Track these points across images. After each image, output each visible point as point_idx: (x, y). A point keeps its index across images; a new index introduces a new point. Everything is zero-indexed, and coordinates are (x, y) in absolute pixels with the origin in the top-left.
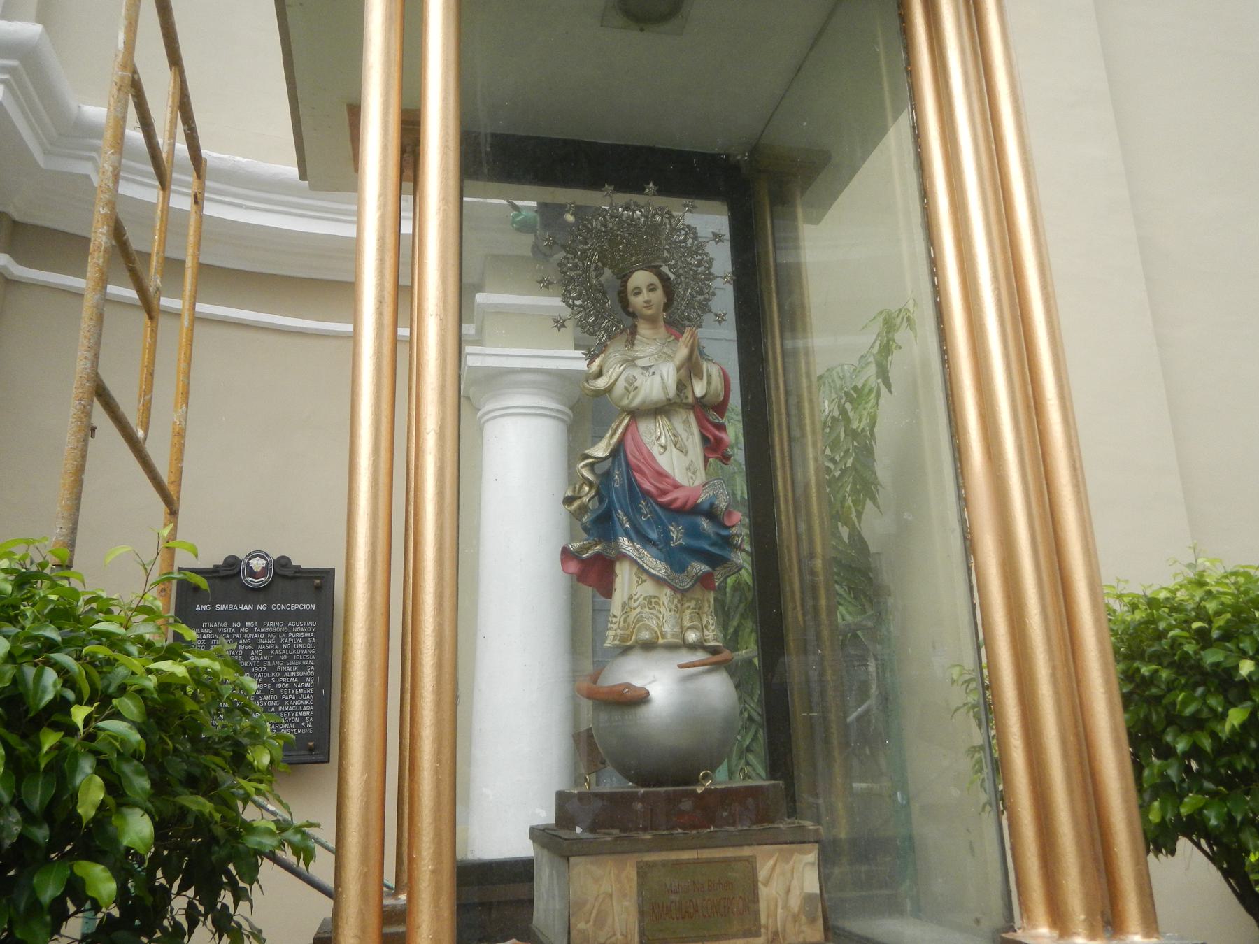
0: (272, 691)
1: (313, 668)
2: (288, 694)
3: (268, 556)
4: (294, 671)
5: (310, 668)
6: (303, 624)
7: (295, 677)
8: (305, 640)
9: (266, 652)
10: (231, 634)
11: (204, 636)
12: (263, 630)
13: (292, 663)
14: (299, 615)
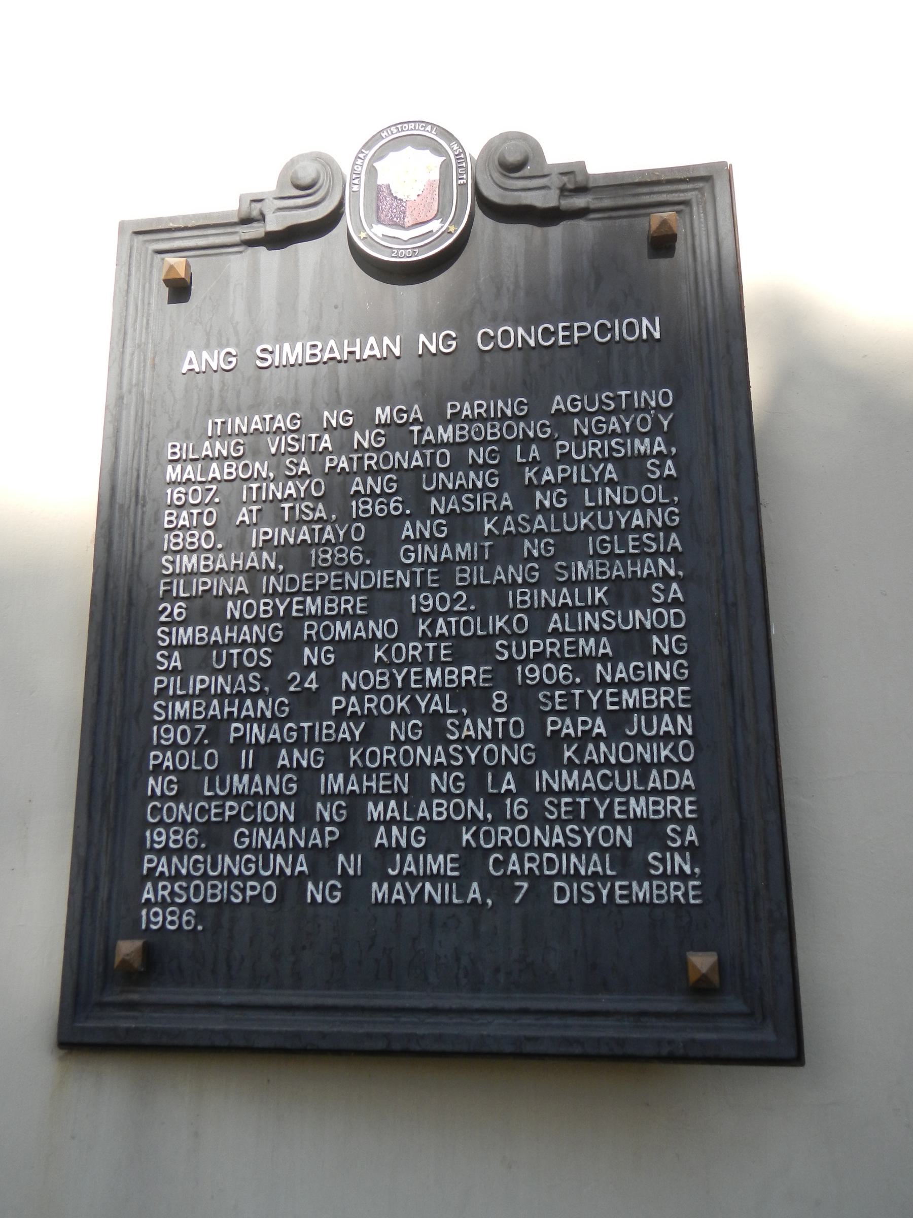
0: (499, 699)
2: (571, 713)
3: (449, 136)
4: (592, 608)
5: (666, 591)
6: (617, 399)
7: (597, 635)
12: (446, 434)
13: (581, 569)
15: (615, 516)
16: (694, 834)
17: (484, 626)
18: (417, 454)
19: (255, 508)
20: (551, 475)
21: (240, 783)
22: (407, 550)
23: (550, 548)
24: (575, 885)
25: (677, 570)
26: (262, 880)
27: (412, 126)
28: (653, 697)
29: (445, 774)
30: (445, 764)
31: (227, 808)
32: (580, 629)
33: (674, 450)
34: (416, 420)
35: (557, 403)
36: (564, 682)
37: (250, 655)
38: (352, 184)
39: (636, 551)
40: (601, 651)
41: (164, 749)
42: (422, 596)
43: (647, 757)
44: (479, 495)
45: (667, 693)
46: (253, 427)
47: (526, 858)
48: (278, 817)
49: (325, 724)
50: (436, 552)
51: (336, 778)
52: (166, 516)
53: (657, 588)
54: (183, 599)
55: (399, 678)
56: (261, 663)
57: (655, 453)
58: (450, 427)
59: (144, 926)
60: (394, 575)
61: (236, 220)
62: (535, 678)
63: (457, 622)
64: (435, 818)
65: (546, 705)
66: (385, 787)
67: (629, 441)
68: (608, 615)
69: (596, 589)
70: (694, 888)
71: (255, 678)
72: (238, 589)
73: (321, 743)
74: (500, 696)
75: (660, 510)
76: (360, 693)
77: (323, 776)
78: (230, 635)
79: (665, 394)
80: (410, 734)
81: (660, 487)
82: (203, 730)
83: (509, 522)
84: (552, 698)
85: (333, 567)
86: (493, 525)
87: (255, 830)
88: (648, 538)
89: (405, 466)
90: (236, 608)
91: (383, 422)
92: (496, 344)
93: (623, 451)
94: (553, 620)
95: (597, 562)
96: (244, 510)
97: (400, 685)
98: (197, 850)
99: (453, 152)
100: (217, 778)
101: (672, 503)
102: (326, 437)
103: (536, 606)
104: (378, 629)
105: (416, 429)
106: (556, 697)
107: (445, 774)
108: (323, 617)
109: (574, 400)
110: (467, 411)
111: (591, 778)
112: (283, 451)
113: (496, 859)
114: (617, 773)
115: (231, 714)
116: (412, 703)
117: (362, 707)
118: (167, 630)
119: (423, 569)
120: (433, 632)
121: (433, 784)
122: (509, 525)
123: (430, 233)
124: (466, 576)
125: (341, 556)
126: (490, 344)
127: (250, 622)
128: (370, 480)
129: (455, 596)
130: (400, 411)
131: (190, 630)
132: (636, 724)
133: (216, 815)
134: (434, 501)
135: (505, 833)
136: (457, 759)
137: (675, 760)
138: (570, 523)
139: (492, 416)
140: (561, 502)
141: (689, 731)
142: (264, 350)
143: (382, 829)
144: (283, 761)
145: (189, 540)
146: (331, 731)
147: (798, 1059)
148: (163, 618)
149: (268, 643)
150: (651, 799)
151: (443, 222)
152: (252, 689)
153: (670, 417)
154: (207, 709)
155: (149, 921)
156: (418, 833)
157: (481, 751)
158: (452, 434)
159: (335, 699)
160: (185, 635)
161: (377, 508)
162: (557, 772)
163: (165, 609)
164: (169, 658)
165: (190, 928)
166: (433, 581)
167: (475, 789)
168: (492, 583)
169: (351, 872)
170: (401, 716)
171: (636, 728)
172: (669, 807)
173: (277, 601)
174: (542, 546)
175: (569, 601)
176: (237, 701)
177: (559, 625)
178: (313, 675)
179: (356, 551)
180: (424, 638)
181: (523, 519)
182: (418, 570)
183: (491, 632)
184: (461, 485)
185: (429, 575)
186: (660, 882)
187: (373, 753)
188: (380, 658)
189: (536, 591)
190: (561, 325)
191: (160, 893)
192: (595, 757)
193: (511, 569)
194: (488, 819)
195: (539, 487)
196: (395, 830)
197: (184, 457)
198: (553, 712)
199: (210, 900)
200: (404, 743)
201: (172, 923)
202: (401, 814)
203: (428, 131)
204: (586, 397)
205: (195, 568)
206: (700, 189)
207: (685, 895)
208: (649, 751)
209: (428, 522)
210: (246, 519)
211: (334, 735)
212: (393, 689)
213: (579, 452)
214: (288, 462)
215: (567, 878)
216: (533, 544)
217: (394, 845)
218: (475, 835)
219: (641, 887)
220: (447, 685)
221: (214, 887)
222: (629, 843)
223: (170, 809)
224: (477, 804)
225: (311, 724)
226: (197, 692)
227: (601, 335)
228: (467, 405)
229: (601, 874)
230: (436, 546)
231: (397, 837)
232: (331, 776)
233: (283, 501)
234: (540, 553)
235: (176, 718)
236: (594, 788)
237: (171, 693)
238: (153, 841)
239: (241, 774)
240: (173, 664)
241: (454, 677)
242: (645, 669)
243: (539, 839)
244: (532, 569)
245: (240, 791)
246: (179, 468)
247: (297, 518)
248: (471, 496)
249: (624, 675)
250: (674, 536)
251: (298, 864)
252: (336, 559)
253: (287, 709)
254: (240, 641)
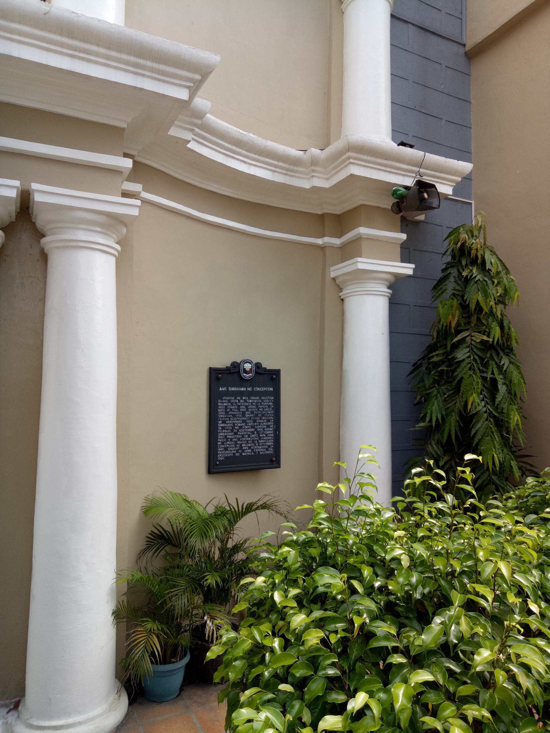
0: (255, 432)
1: (273, 421)
2: (262, 434)
8: (269, 406)
9: (252, 412)
10: (236, 403)
11: (224, 404)
12: (250, 401)
14: (266, 393)
21: (228, 443)
147: (280, 467)
160: (222, 425)
167: (253, 442)
170: (246, 435)
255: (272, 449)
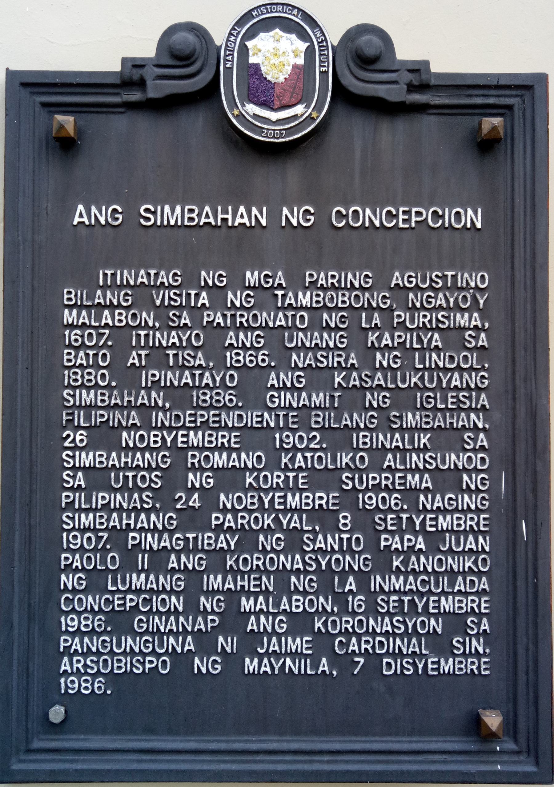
2: (401, 532)
4: (418, 450)
5: (475, 440)
7: (422, 472)
11: (107, 317)
12: (305, 299)
13: (410, 419)
15: (439, 377)
16: (487, 625)
17: (334, 460)
18: (281, 315)
19: (143, 353)
20: (389, 340)
21: (138, 581)
22: (272, 396)
23: (386, 400)
24: (399, 661)
25: (484, 424)
26: (159, 656)
27: (280, 8)
28: (462, 522)
29: (302, 577)
30: (302, 569)
31: (128, 601)
32: (408, 467)
33: (487, 325)
34: (280, 285)
35: (396, 279)
36: (394, 508)
37: (143, 477)
38: (226, 60)
39: (454, 407)
40: (424, 485)
41: (73, 552)
42: (284, 435)
43: (455, 568)
44: (331, 353)
45: (472, 519)
46: (140, 280)
47: (363, 641)
48: (170, 608)
49: (206, 536)
50: (296, 399)
51: (215, 578)
52: (65, 355)
53: (469, 437)
54: (84, 428)
55: (266, 501)
56: (153, 485)
57: (472, 326)
58: (308, 293)
59: (63, 691)
60: (262, 416)
61: (118, 81)
62: (372, 504)
63: (312, 457)
64: (294, 610)
65: (380, 525)
66: (255, 586)
67: (452, 314)
68: (431, 457)
69: (422, 435)
70: (485, 663)
71: (147, 496)
72: (131, 421)
73: (203, 550)
74: (345, 517)
75: (473, 374)
76: (235, 512)
77: (205, 577)
78: (126, 460)
79: (483, 277)
80: (274, 545)
81: (475, 355)
82: (105, 538)
83: (355, 377)
84: (385, 520)
85: (212, 407)
86: (342, 379)
87: (151, 618)
88: (464, 396)
89: (271, 324)
90: (130, 438)
91: (252, 285)
92: (347, 222)
93: (447, 323)
94: (388, 459)
95: (424, 413)
96: (134, 353)
97: (266, 506)
98: (105, 632)
99: (317, 38)
100: (119, 576)
101: (483, 369)
102: (204, 294)
103: (374, 447)
104: (249, 460)
105: (280, 293)
106: (389, 519)
107: (302, 577)
108: (204, 449)
109: (410, 276)
110: (322, 280)
111: (413, 582)
112: (166, 304)
113: (341, 641)
114: (432, 578)
115: (128, 525)
116: (277, 520)
117: (236, 522)
118: (71, 454)
119: (285, 413)
120: (293, 464)
121: (292, 585)
122: (355, 380)
123: (295, 117)
124: (320, 420)
125: (218, 398)
126: (342, 221)
127: (143, 450)
128: (241, 336)
129: (311, 436)
130: (266, 276)
131: (91, 454)
132: (448, 542)
133: (119, 605)
134: (294, 357)
135: (347, 622)
136: (311, 566)
137: (476, 570)
138: (404, 381)
139: (343, 286)
140: (396, 363)
141: (487, 549)
142: (147, 210)
143: (253, 618)
144: (173, 563)
145: (87, 377)
146: (211, 542)
148: (67, 444)
149: (158, 468)
150: (457, 598)
151: (307, 107)
152: (145, 506)
153: (485, 297)
154: (108, 520)
155: (67, 687)
156: (281, 621)
157: (330, 559)
158: (310, 300)
159: (214, 515)
161: (248, 359)
162: (387, 577)
163: (68, 436)
164: (74, 477)
165: (101, 692)
166: (293, 423)
168: (340, 426)
169: (228, 650)
171: (448, 545)
172: (469, 605)
173: (165, 433)
174: (380, 398)
175: (400, 444)
176: (133, 515)
177: (392, 463)
178: (196, 496)
179: (231, 394)
180: (287, 468)
181: (366, 375)
182: (281, 413)
183: (339, 467)
184: (316, 344)
185: (290, 418)
186: (460, 659)
187: (245, 560)
188: (250, 483)
189: (374, 435)
190: (401, 209)
191: (75, 666)
192: (416, 567)
193: (355, 416)
194: (334, 611)
195: (380, 349)
196: (263, 619)
197: (79, 303)
198: (386, 530)
199: (116, 671)
200: (269, 552)
201: (86, 688)
202: (268, 606)
203: (294, 15)
204: (419, 275)
205: (93, 402)
206: (521, 96)
207: (479, 668)
208: (456, 563)
209: (290, 373)
210: (136, 361)
211: (214, 545)
212: (261, 509)
213: (412, 321)
214: (171, 314)
215: (393, 655)
216: (373, 395)
217: (262, 630)
218: (325, 624)
219: (447, 662)
220: (303, 508)
221: (119, 661)
222: (439, 631)
223: (80, 600)
224: (327, 600)
225: (195, 535)
226: (99, 507)
227: (435, 221)
228: (322, 275)
229: (418, 653)
230: (296, 394)
231: (264, 624)
232: (212, 577)
233: (168, 347)
234: (378, 404)
235: (82, 527)
236: (415, 589)
237: (77, 506)
238: (67, 625)
239: (139, 573)
240: (77, 483)
241: (310, 501)
242: (457, 500)
243: (373, 627)
244: (372, 417)
245: (138, 588)
246: (75, 312)
247: (180, 364)
248: (325, 354)
249: (441, 505)
250: (483, 396)
251: (187, 644)
252: (214, 401)
253: (175, 523)
254: (134, 466)
255: (479, 646)
